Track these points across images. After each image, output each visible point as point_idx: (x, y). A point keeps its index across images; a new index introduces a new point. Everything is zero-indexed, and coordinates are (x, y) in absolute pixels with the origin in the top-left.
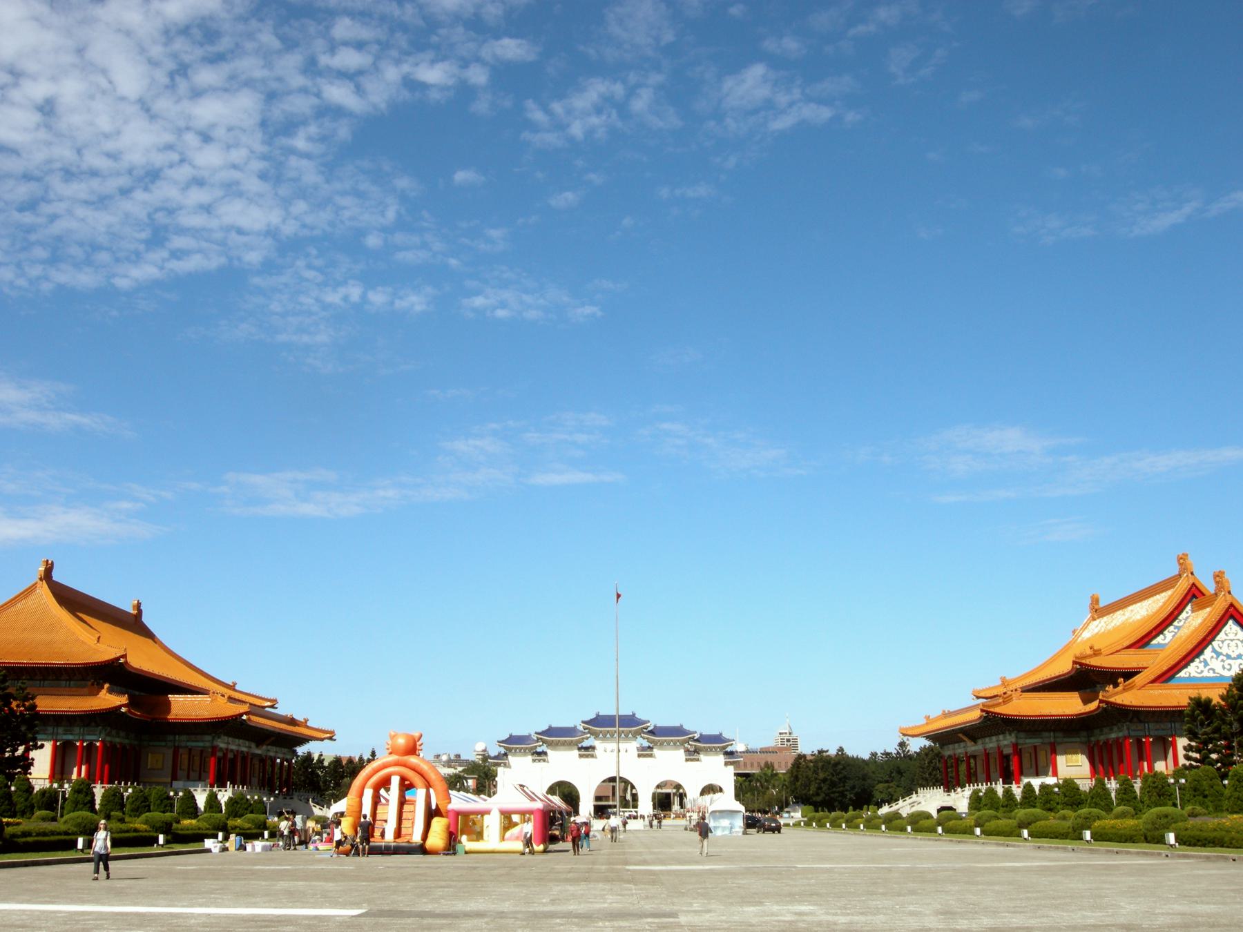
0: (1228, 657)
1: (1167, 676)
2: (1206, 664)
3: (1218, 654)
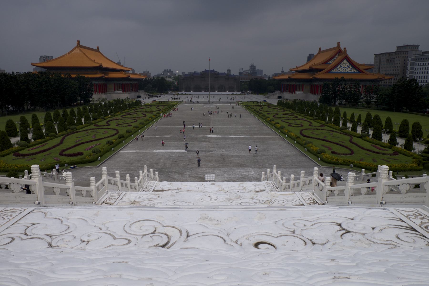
0: (343, 67)
1: (329, 71)
2: (338, 69)
3: (341, 67)
